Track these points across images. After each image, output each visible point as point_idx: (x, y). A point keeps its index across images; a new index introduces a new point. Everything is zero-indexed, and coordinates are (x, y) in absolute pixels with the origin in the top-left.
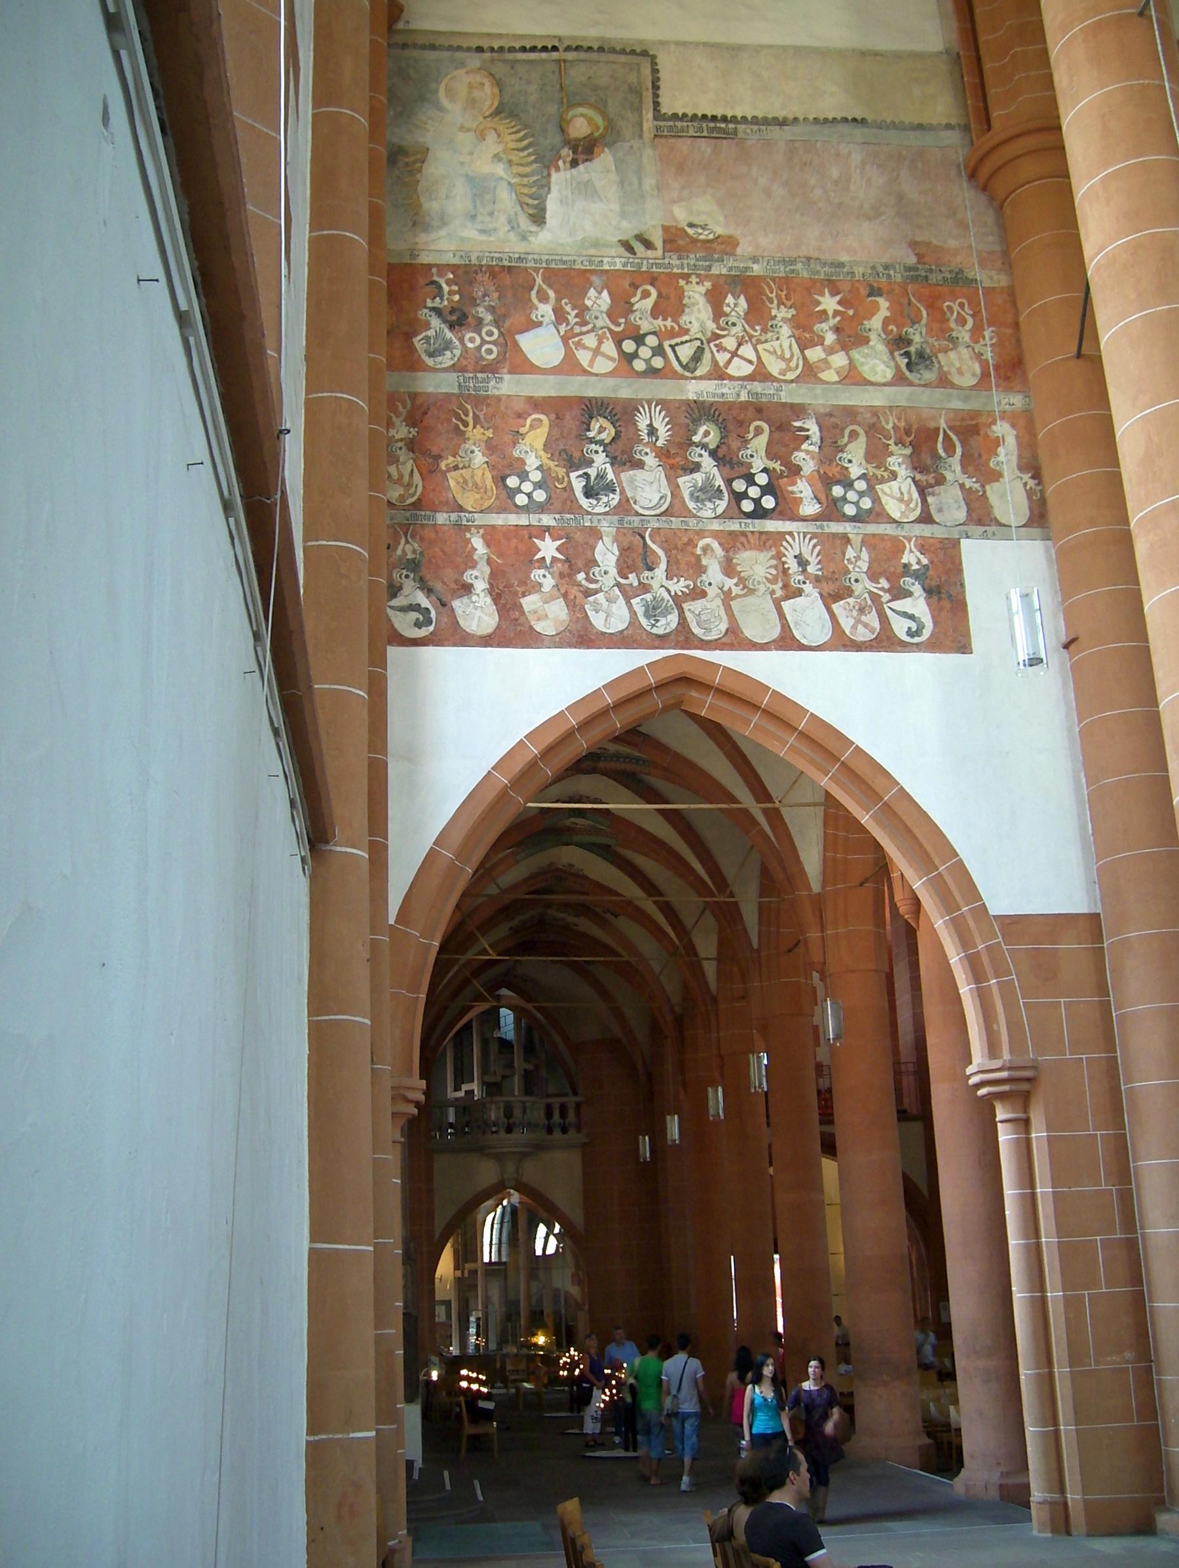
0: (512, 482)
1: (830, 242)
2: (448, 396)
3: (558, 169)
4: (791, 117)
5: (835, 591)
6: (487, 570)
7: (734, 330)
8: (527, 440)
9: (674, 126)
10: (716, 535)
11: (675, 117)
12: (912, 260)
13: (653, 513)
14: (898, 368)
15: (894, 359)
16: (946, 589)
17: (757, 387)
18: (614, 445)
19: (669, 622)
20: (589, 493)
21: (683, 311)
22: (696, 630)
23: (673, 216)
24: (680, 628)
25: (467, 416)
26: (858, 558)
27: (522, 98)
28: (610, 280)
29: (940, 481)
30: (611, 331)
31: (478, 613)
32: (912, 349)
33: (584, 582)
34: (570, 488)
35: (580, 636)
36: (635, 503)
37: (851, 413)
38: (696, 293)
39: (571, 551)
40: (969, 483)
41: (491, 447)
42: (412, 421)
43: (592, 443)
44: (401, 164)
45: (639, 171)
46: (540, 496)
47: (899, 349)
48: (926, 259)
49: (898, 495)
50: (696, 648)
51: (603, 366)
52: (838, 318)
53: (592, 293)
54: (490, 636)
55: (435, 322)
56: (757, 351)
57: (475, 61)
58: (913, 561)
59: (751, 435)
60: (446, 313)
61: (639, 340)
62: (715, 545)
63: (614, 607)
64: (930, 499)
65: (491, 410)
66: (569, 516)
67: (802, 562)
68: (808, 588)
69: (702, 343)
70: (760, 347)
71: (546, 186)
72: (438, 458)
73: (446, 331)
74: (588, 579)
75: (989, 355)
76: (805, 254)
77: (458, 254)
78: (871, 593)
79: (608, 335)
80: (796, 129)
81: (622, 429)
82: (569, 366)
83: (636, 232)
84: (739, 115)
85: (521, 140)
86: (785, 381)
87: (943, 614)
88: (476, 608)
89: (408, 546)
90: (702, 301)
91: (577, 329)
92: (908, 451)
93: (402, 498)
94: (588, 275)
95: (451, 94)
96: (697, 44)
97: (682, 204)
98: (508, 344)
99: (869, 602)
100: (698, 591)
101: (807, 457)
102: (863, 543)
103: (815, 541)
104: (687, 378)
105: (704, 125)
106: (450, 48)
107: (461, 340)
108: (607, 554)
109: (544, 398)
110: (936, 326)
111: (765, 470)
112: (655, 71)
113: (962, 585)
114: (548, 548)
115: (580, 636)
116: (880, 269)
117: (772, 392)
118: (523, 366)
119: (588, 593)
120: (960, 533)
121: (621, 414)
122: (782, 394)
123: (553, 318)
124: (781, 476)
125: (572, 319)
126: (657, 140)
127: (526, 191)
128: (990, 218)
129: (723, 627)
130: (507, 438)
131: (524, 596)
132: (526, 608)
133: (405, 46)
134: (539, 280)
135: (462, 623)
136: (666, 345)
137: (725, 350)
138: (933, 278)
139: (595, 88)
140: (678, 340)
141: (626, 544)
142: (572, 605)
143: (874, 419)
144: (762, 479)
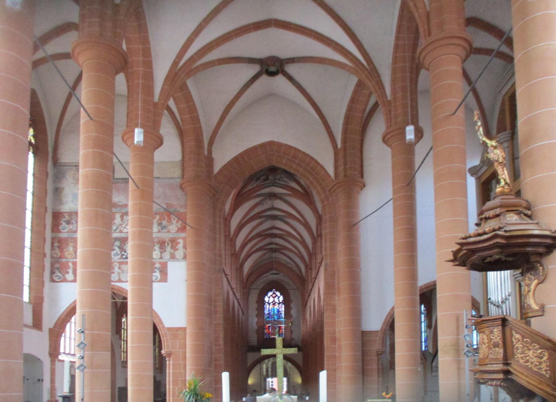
2: (66, 238)
42: (58, 242)
62: (117, 264)
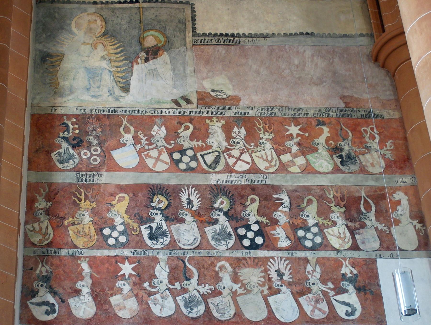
0: (107, 231)
2: (70, 184)
3: (137, 63)
4: (271, 33)
5: (300, 290)
6: (90, 281)
7: (238, 146)
8: (116, 208)
9: (203, 40)
10: (228, 259)
11: (205, 35)
12: (342, 105)
13: (189, 248)
14: (335, 164)
15: (333, 159)
17: (252, 176)
20: (152, 237)
21: (208, 137)
22: (216, 314)
23: (203, 87)
24: (206, 313)
25: (81, 195)
26: (314, 271)
27: (118, 28)
28: (166, 121)
29: (363, 226)
30: (166, 148)
31: (84, 306)
32: (344, 154)
33: (148, 288)
34: (140, 235)
35: (145, 319)
37: (308, 189)
39: (141, 270)
40: (380, 227)
41: (94, 212)
42: (48, 198)
43: (154, 209)
44: (48, 62)
45: (184, 63)
46: (123, 239)
47: (336, 153)
48: (351, 105)
49: (338, 234)
52: (299, 138)
53: (156, 128)
54: (90, 319)
55: (64, 145)
56: (251, 157)
57: (92, 9)
58: (348, 272)
59: (248, 203)
61: (183, 152)
62: (227, 265)
63: (166, 302)
64: (357, 237)
65: (95, 192)
66: (140, 250)
67: (280, 274)
68: (284, 289)
69: (219, 153)
70: (253, 155)
72: (63, 218)
73: (71, 149)
74: (150, 286)
75: (389, 155)
76: (280, 104)
77: (80, 108)
78: (322, 291)
79: (164, 150)
80: (274, 39)
81: (172, 201)
82: (142, 167)
83: (181, 95)
84: (241, 33)
85: (117, 48)
86: (269, 173)
87: (367, 302)
88: (82, 303)
90: (219, 131)
91: (147, 147)
92: (343, 210)
93: (41, 241)
94: (154, 118)
95: (78, 26)
97: (209, 79)
98: (106, 156)
99: (322, 296)
100: (217, 291)
101: (282, 215)
102: (317, 262)
103: (288, 262)
104: (210, 173)
105: (221, 39)
107: (79, 154)
108: (162, 272)
109: (126, 185)
111: (257, 222)
112: (193, 12)
113: (379, 285)
114: (127, 269)
115: (145, 319)
116: (324, 111)
117: (261, 179)
118: (115, 168)
119: (150, 294)
120: (376, 255)
121: (171, 193)
122: (267, 180)
123: (133, 141)
124: (267, 225)
125: (144, 141)
127: (119, 75)
128: (387, 82)
129: (232, 312)
130: (104, 207)
131: (112, 295)
134: (125, 122)
135: (74, 312)
136: (198, 155)
137: (233, 157)
138: (354, 115)
139: (159, 22)
141: (173, 266)
142: (141, 301)
144: (255, 227)
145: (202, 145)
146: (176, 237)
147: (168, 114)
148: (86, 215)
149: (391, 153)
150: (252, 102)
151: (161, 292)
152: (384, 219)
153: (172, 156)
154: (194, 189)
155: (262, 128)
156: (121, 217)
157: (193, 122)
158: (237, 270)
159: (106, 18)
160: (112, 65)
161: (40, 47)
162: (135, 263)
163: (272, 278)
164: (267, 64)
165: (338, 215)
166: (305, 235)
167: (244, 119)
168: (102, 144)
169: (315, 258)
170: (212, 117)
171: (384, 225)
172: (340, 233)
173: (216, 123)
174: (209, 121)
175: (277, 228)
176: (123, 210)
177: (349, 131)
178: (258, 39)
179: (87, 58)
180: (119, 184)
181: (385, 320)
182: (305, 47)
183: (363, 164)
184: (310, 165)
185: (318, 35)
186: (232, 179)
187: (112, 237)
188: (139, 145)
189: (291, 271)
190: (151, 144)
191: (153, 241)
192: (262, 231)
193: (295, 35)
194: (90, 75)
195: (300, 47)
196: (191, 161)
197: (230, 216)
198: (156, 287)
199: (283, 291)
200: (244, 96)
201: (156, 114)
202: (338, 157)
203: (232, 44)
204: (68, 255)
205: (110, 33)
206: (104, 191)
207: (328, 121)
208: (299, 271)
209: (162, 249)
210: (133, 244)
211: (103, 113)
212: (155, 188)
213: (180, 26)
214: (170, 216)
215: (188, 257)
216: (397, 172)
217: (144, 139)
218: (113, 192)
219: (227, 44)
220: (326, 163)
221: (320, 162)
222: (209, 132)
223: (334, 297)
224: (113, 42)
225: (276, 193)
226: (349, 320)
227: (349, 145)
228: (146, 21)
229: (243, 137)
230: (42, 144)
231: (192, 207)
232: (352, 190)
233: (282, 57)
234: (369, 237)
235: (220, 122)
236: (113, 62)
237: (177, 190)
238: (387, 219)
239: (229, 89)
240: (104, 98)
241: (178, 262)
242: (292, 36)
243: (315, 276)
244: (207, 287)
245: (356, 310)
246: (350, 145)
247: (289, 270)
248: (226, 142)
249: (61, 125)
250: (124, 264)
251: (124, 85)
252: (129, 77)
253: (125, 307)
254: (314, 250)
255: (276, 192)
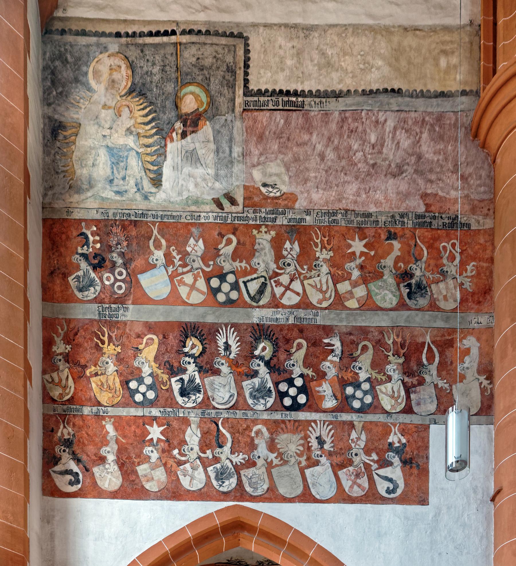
0: (133, 385)
1: (364, 196)
2: (92, 321)
3: (172, 140)
4: (345, 89)
5: (341, 461)
6: (116, 447)
10: (265, 422)
11: (260, 93)
12: (422, 209)
14: (401, 295)
15: (399, 289)
16: (415, 462)
17: (301, 313)
18: (201, 358)
19: (230, 484)
20: (183, 393)
21: (254, 255)
22: (248, 489)
23: (252, 178)
24: (238, 487)
25: (104, 336)
26: (358, 439)
27: (148, 79)
29: (421, 382)
30: (203, 271)
31: (109, 476)
33: (178, 456)
34: (170, 390)
36: (213, 400)
37: (364, 331)
38: (264, 239)
39: (170, 434)
41: (120, 359)
42: (67, 341)
43: (186, 356)
44: (61, 137)
46: (151, 395)
48: (433, 208)
49: (390, 394)
50: (247, 501)
51: (197, 298)
52: (363, 258)
53: (192, 241)
54: (116, 492)
55: (84, 265)
57: (114, 45)
58: (396, 440)
59: (293, 350)
60: (91, 258)
61: (222, 278)
62: (264, 430)
63: (196, 473)
64: (412, 396)
65: (120, 332)
67: (321, 442)
69: (266, 280)
70: (306, 282)
71: (162, 154)
72: (85, 367)
73: (91, 271)
74: (180, 454)
75: (468, 285)
76: (344, 206)
77: (101, 210)
78: (365, 464)
79: (201, 274)
80: (349, 100)
81: (207, 346)
82: (174, 299)
83: (225, 192)
85: (147, 115)
86: (321, 309)
87: (412, 478)
89: (65, 430)
90: (267, 246)
91: (180, 270)
92: (401, 360)
94: (190, 227)
95: (97, 74)
96: (280, 25)
97: (260, 167)
98: (132, 281)
100: (251, 461)
101: (331, 366)
102: (363, 427)
103: (331, 426)
104: (253, 307)
106: (96, 34)
108: (193, 437)
109: (155, 322)
110: (432, 262)
111: (302, 376)
112: (247, 51)
113: (427, 458)
114: (155, 432)
115: (174, 493)
116: (398, 217)
117: (311, 317)
118: (143, 299)
119: (180, 463)
120: (430, 420)
121: (206, 333)
122: (318, 318)
123: (164, 261)
125: (177, 262)
126: (245, 113)
127: (149, 159)
129: (266, 487)
130: (131, 352)
131: (139, 464)
132: (140, 473)
133: (63, 32)
134: (155, 232)
135: (99, 482)
136: (241, 281)
140: (249, 278)
141: (205, 430)
142: (169, 472)
143: (380, 337)
144: (299, 382)
145: (246, 267)
146: (210, 394)
147: (207, 221)
148: (110, 363)
149: (470, 282)
150: (311, 203)
151: (192, 461)
152: (447, 374)
153: (209, 283)
154: (233, 329)
155: (319, 244)
156: (149, 367)
157: (237, 233)
158: (274, 436)
159: (133, 62)
160: (141, 143)
161: (49, 111)
162: (164, 426)
163: (312, 446)
164: (336, 142)
165: (395, 367)
166: (354, 393)
167: (299, 229)
168: (128, 265)
169: (362, 423)
170: (260, 226)
171: (445, 381)
172: (393, 392)
173: (265, 235)
174: (257, 231)
175: (324, 383)
176: (151, 357)
177: (424, 249)
178: (328, 100)
179: (109, 130)
180: (147, 322)
181: (428, 499)
182: (388, 113)
183: (435, 296)
184: (371, 297)
185: (407, 93)
186: (278, 316)
187: (139, 392)
188: (171, 267)
189: (333, 438)
190: (185, 265)
191: (184, 398)
192: (306, 387)
193: (376, 93)
194: (113, 160)
195: (381, 114)
196: (231, 290)
197: (271, 367)
198: (185, 455)
199: (322, 463)
200: (302, 193)
201: (193, 221)
202: (405, 286)
203: (294, 108)
204: (91, 414)
205: (138, 89)
206: (130, 330)
207: (401, 233)
208: (342, 439)
209: (194, 408)
210: (162, 401)
211: (129, 219)
212: (189, 326)
213: (228, 76)
214: (205, 366)
215: (221, 419)
216: (473, 308)
217: (178, 257)
218: (140, 333)
219: (288, 108)
220: (390, 296)
221: (383, 293)
222: (255, 248)
223: (376, 471)
224: (141, 104)
225: (328, 336)
226: (389, 498)
227: (421, 269)
228: (185, 69)
229: (295, 256)
230: (58, 263)
231: (230, 354)
232: (416, 333)
233: (356, 131)
234: (426, 397)
235: (270, 234)
236: (142, 138)
237: (213, 330)
238: (450, 374)
239: (284, 183)
240: (130, 195)
241: (210, 425)
242: (373, 95)
243: (359, 445)
244: (241, 456)
245: (398, 487)
246: (423, 270)
247: (332, 437)
248: (275, 263)
249: (78, 236)
250: (152, 426)
251: (155, 176)
252: (161, 162)
253: (153, 479)
254: (362, 412)
255: (328, 336)
